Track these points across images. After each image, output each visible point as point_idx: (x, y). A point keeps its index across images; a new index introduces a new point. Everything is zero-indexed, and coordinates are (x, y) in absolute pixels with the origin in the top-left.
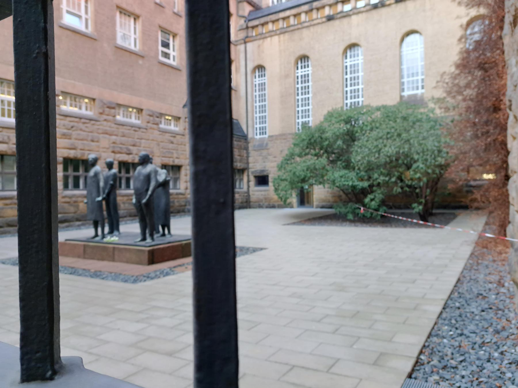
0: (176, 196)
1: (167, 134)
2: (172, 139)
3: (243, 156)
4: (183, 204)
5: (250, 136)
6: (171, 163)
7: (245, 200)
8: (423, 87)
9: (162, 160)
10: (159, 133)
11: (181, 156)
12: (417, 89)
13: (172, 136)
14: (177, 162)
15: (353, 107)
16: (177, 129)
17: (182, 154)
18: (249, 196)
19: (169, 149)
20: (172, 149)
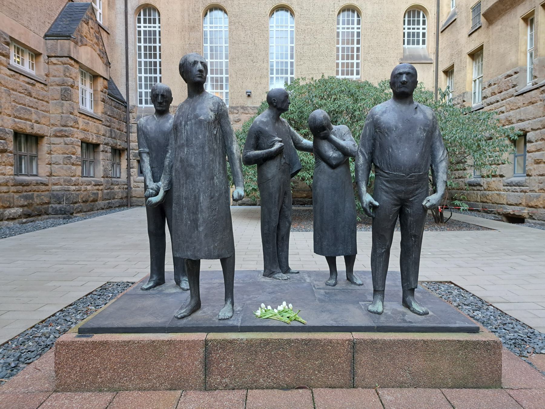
0: (35, 188)
1: (22, 78)
2: (29, 87)
3: (123, 131)
4: (46, 200)
5: (131, 103)
6: (29, 130)
7: (125, 195)
8: (358, 73)
9: (15, 121)
10: (9, 72)
11: (43, 121)
12: (352, 74)
13: (28, 83)
14: (37, 129)
15: (289, 83)
16: (33, 73)
17: (45, 117)
18: (129, 188)
19: (25, 105)
20: (29, 106)
